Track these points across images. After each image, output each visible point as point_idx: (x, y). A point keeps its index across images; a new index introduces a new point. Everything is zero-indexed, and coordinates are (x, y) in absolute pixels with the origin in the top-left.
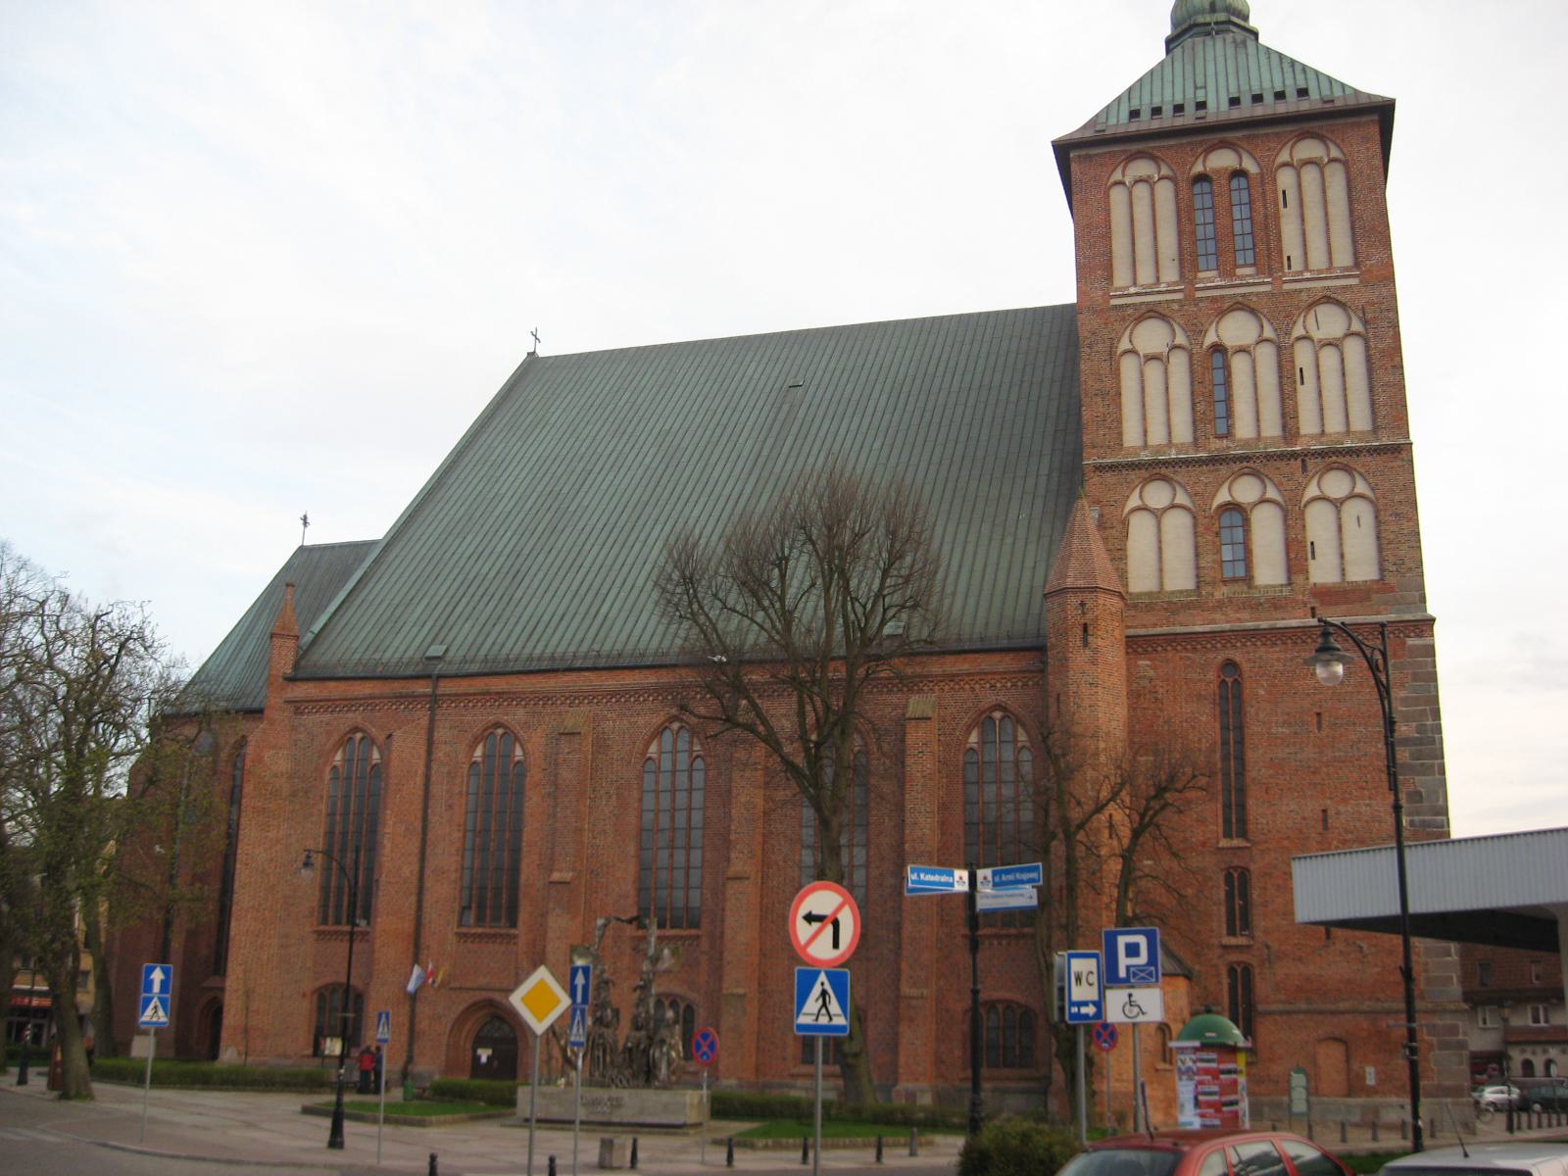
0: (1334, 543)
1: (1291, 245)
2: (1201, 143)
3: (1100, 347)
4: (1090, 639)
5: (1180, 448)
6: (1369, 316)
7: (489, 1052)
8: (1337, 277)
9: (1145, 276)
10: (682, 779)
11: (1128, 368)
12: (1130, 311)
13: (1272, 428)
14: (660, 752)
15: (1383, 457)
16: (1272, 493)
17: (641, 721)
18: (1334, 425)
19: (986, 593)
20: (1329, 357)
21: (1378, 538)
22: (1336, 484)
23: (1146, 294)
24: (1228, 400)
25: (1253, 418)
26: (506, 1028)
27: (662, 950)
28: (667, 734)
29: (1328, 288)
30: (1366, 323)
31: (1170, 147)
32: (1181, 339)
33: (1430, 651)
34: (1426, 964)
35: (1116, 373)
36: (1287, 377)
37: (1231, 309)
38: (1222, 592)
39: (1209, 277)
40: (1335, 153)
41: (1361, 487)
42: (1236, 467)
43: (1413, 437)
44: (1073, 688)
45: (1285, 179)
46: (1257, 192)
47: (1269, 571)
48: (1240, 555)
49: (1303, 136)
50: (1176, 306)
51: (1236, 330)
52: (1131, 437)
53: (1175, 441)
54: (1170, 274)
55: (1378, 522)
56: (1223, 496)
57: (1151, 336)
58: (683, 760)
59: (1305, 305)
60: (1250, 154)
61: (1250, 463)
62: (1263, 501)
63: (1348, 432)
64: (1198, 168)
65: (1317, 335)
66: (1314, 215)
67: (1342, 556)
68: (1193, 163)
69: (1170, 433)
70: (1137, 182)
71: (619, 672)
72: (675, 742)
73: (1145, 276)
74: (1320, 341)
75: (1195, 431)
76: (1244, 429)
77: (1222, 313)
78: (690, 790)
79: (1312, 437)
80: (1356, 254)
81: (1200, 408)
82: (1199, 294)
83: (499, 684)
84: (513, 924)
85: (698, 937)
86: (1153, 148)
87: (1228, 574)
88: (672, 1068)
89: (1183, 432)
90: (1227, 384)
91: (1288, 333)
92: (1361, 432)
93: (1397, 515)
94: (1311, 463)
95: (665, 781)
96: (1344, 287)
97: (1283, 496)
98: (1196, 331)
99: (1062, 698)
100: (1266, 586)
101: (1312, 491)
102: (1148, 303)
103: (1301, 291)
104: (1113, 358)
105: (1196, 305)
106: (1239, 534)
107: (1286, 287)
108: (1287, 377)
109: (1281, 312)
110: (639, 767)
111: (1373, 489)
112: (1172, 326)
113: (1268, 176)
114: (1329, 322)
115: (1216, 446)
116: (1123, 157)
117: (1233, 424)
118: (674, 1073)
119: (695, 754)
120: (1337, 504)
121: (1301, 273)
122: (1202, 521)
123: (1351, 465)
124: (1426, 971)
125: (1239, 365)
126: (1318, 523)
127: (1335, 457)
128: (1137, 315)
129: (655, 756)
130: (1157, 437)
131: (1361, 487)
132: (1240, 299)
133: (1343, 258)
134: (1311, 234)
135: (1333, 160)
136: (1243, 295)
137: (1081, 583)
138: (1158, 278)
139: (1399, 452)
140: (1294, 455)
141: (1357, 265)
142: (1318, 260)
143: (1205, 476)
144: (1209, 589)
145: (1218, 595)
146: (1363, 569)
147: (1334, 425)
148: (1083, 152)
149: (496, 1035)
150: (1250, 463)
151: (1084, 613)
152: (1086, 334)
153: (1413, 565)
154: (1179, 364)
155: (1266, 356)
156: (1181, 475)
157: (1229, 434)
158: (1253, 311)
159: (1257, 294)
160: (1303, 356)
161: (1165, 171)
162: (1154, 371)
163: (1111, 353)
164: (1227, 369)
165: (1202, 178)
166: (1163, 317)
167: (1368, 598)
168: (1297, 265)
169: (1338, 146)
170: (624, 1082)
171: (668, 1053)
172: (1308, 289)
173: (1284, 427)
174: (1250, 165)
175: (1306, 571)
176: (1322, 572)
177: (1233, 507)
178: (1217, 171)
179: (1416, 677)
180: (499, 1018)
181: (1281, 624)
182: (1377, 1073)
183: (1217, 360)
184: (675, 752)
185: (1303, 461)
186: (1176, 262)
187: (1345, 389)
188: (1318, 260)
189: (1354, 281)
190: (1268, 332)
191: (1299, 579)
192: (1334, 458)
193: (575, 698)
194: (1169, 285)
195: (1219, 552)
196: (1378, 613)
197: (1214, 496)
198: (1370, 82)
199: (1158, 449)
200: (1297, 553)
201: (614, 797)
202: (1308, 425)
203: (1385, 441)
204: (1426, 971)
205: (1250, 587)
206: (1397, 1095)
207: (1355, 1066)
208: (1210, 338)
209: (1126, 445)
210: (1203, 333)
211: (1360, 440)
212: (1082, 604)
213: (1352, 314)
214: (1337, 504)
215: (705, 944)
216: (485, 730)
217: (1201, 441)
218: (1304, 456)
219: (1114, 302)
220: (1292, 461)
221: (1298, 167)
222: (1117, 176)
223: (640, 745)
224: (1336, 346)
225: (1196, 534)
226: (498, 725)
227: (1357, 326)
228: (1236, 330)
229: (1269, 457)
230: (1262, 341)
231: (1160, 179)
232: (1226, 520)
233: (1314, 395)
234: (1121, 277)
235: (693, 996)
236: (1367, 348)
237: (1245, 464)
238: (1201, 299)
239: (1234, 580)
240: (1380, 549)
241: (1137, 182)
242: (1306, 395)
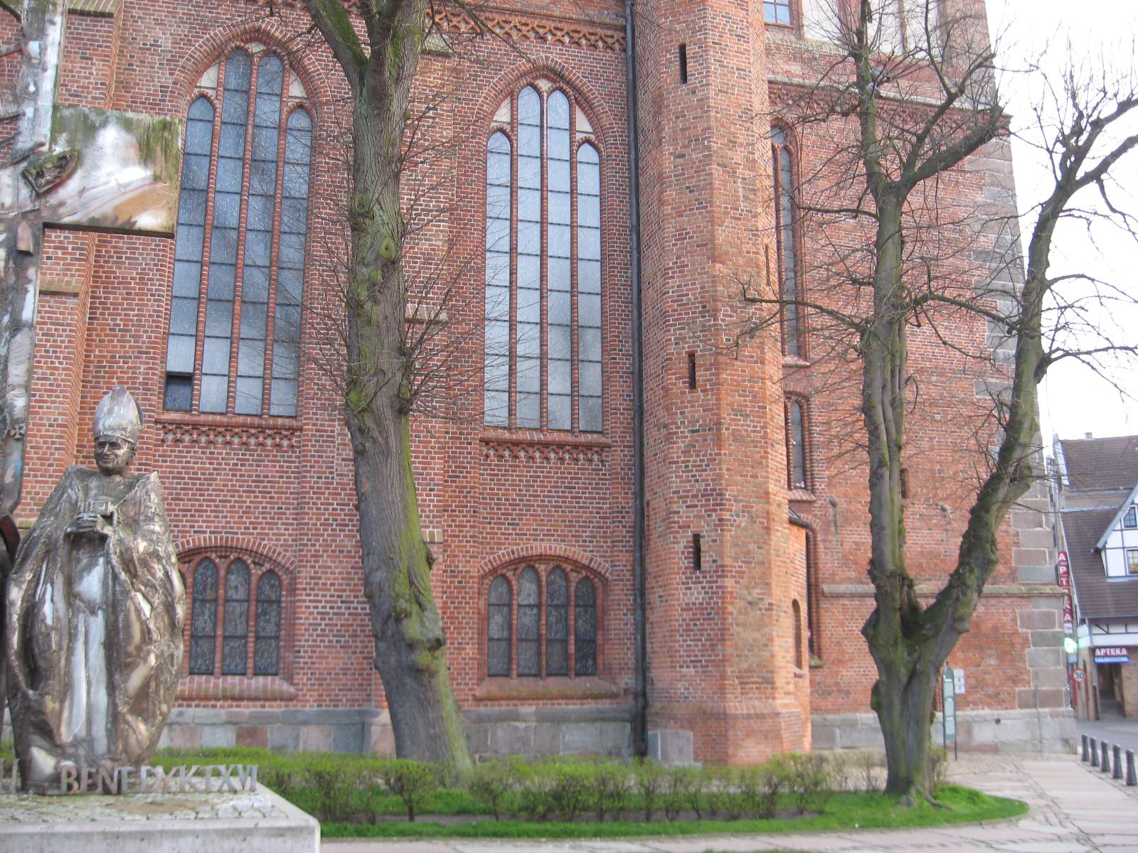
27: (90, 130)
34: (1017, 534)
44: (712, 37)
88: (136, 679)
118: (142, 703)
124: (1017, 544)
171: (114, 607)
182: (967, 677)
204: (1017, 544)
205: (800, 37)
206: (990, 706)
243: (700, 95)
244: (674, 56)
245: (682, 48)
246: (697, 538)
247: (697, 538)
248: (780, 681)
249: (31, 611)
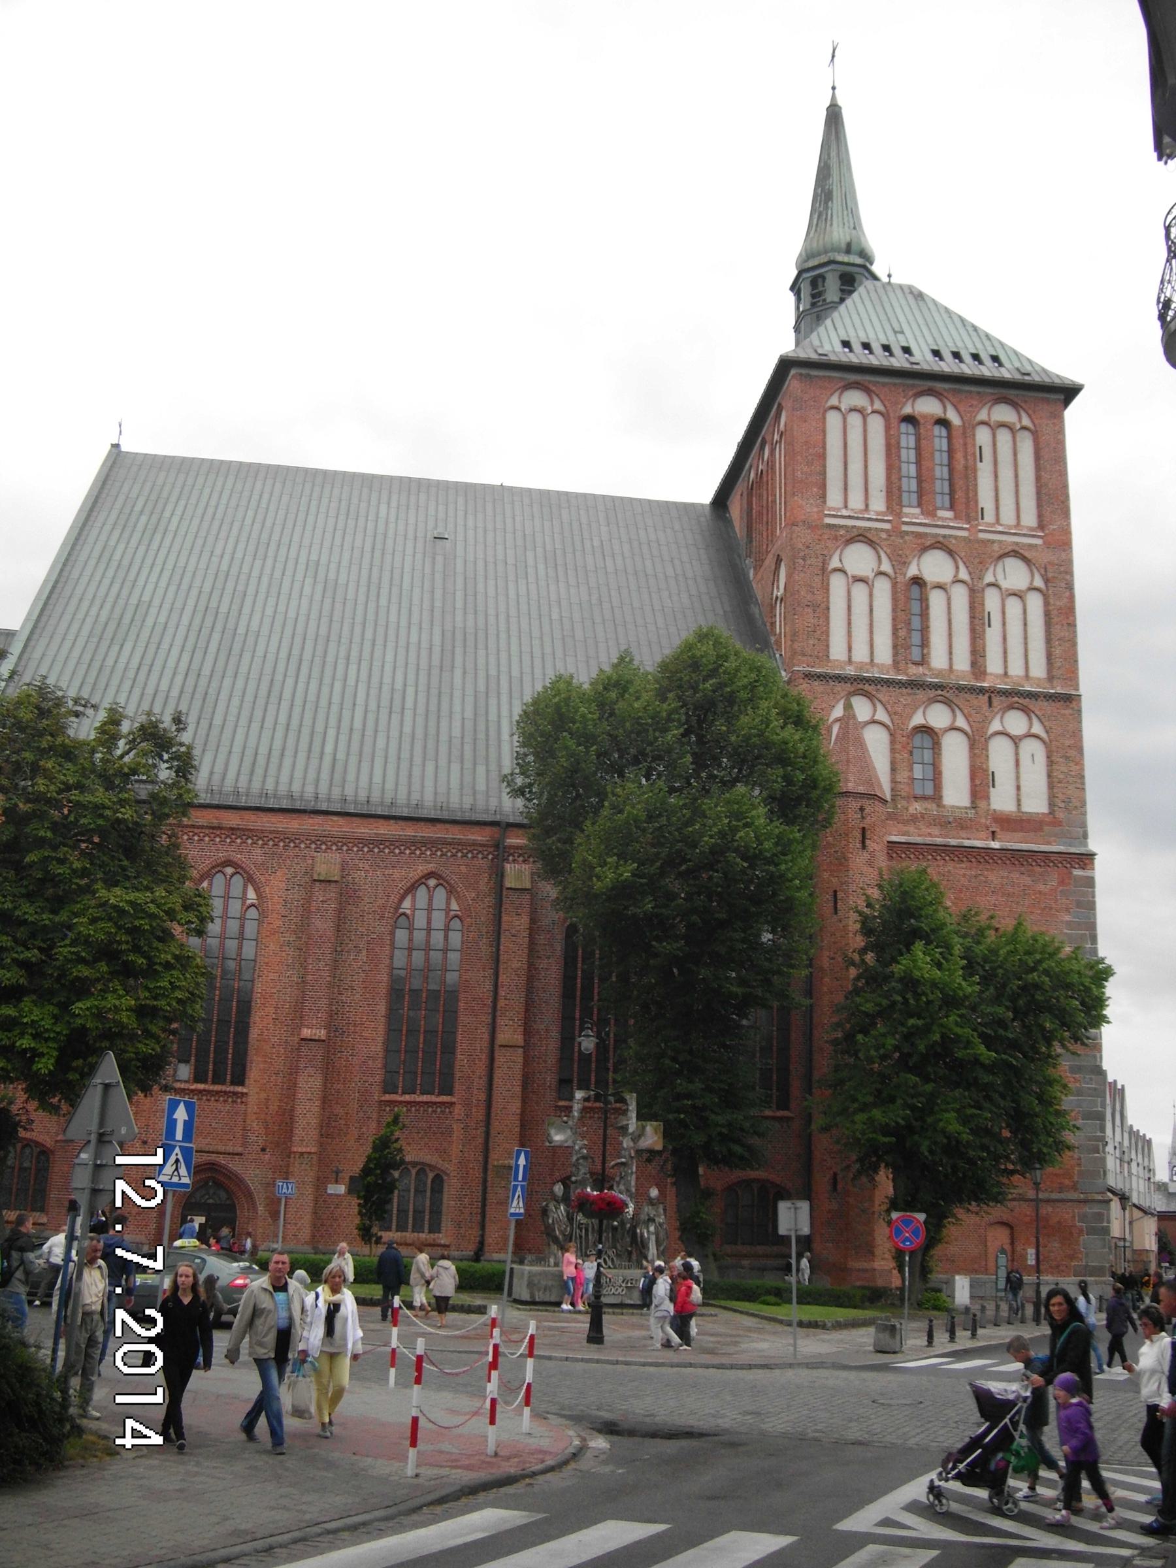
0: (1013, 775)
1: (985, 499)
2: (913, 386)
3: (813, 561)
4: (868, 842)
5: (881, 667)
6: (1050, 575)
7: (203, 1220)
8: (1024, 535)
9: (856, 501)
10: (437, 938)
11: (837, 584)
12: (842, 532)
13: (962, 663)
14: (414, 909)
15: (1055, 703)
16: (961, 722)
17: (396, 874)
18: (1016, 670)
19: (237, 749)
20: (1013, 605)
21: (1049, 776)
22: (1016, 723)
23: (858, 518)
24: (925, 630)
25: (947, 653)
26: (223, 1195)
28: (422, 892)
29: (1017, 544)
30: (1047, 581)
31: (884, 385)
32: (886, 567)
33: (1090, 882)
34: (1080, 1159)
35: (826, 588)
36: (978, 620)
37: (932, 547)
38: (916, 807)
39: (912, 513)
40: (1026, 421)
41: (1037, 728)
42: (932, 693)
43: (1083, 690)
45: (983, 436)
46: (958, 443)
47: (956, 794)
48: (930, 776)
49: (930, 392)
50: (884, 536)
51: (934, 567)
52: (837, 651)
53: (854, 659)
54: (878, 504)
55: (1050, 763)
56: (917, 720)
57: (859, 559)
58: (438, 920)
59: (997, 555)
60: (955, 406)
61: (944, 691)
62: (954, 728)
63: (1027, 676)
64: (907, 410)
65: (1004, 584)
66: (1006, 473)
67: (1018, 788)
68: (905, 404)
69: (872, 653)
70: (851, 410)
71: (372, 820)
72: (431, 899)
73: (856, 501)
74: (1007, 590)
75: (895, 655)
76: (938, 660)
77: (925, 549)
78: (445, 951)
79: (997, 676)
80: (1040, 516)
81: (902, 633)
82: (905, 528)
83: (232, 820)
84: (239, 1079)
85: (452, 1104)
86: (870, 382)
87: (918, 791)
89: (884, 655)
90: (924, 614)
91: (981, 578)
92: (1039, 679)
93: (1067, 758)
94: (996, 700)
95: (420, 937)
96: (1030, 545)
97: (971, 727)
98: (900, 562)
99: (840, 895)
100: (953, 807)
101: (995, 726)
102: (859, 528)
103: (993, 542)
104: (824, 572)
105: (902, 537)
106: (928, 756)
107: (981, 536)
108: (978, 620)
109: (977, 556)
110: (391, 922)
111: (1047, 732)
112: (878, 553)
113: (969, 429)
114: (1014, 575)
115: (915, 671)
116: (842, 384)
117: (929, 653)
119: (452, 913)
120: (1016, 741)
121: (993, 525)
122: (900, 739)
123: (1031, 707)
124: (1079, 1165)
125: (936, 600)
126: (999, 755)
127: (1017, 698)
128: (848, 537)
129: (408, 912)
130: (861, 654)
131: (1037, 728)
132: (941, 539)
133: (1029, 518)
134: (1003, 491)
135: (1024, 428)
136: (944, 536)
137: (861, 789)
138: (867, 506)
139: (1069, 700)
140: (982, 691)
141: (1041, 526)
142: (1008, 517)
143: (904, 697)
144: (904, 803)
145: (911, 810)
146: (1036, 803)
147: (1016, 670)
148: (804, 371)
149: (211, 1201)
150: (944, 691)
151: (863, 818)
152: (800, 546)
153: (1078, 804)
154: (883, 589)
155: (960, 595)
156: (883, 693)
157: (924, 661)
158: (951, 553)
159: (956, 537)
160: (992, 601)
161: (878, 405)
162: (860, 591)
163: (823, 569)
164: (924, 602)
165: (910, 419)
166: (871, 543)
167: (1041, 830)
168: (989, 517)
169: (1030, 416)
170: (610, 1263)
172: (1000, 542)
173: (974, 664)
174: (953, 416)
175: (987, 797)
176: (1001, 800)
177: (925, 730)
178: (925, 416)
179: (1079, 904)
180: (218, 1185)
181: (967, 843)
183: (915, 590)
184: (430, 909)
185: (990, 698)
186: (884, 494)
187: (1026, 638)
188: (1008, 517)
189: (1039, 542)
190: (964, 574)
191: (982, 804)
192: (1016, 699)
193: (321, 842)
194: (878, 513)
195: (911, 770)
196: (1049, 843)
197: (910, 717)
198: (1058, 365)
199: (861, 666)
200: (981, 780)
201: (364, 952)
202: (994, 665)
203: (1059, 690)
204: (1079, 1165)
205: (940, 805)
206: (1052, 1274)
207: (1019, 1249)
208: (912, 571)
209: (831, 658)
210: (906, 564)
211: (1038, 686)
212: (862, 809)
213: (1035, 571)
214: (1016, 741)
215: (458, 1110)
216: (213, 867)
217: (902, 665)
218: (991, 693)
219: (828, 521)
220: (980, 696)
221: (995, 427)
222: (834, 401)
223: (394, 898)
224: (1020, 597)
225: (893, 751)
226: (228, 863)
227: (1039, 582)
228: (934, 567)
229: (960, 689)
230: (957, 581)
231: (873, 412)
232: (918, 740)
233: (999, 639)
234: (834, 498)
235: (445, 1166)
236: (1046, 604)
237: (939, 692)
238: (907, 533)
239: (925, 798)
240: (1051, 786)
241: (851, 410)
242: (992, 636)
243: (844, 923)
244: (829, 897)
245: (835, 892)
246: (835, 1174)
247: (835, 1174)
248: (878, 1252)
249: (642, 1234)
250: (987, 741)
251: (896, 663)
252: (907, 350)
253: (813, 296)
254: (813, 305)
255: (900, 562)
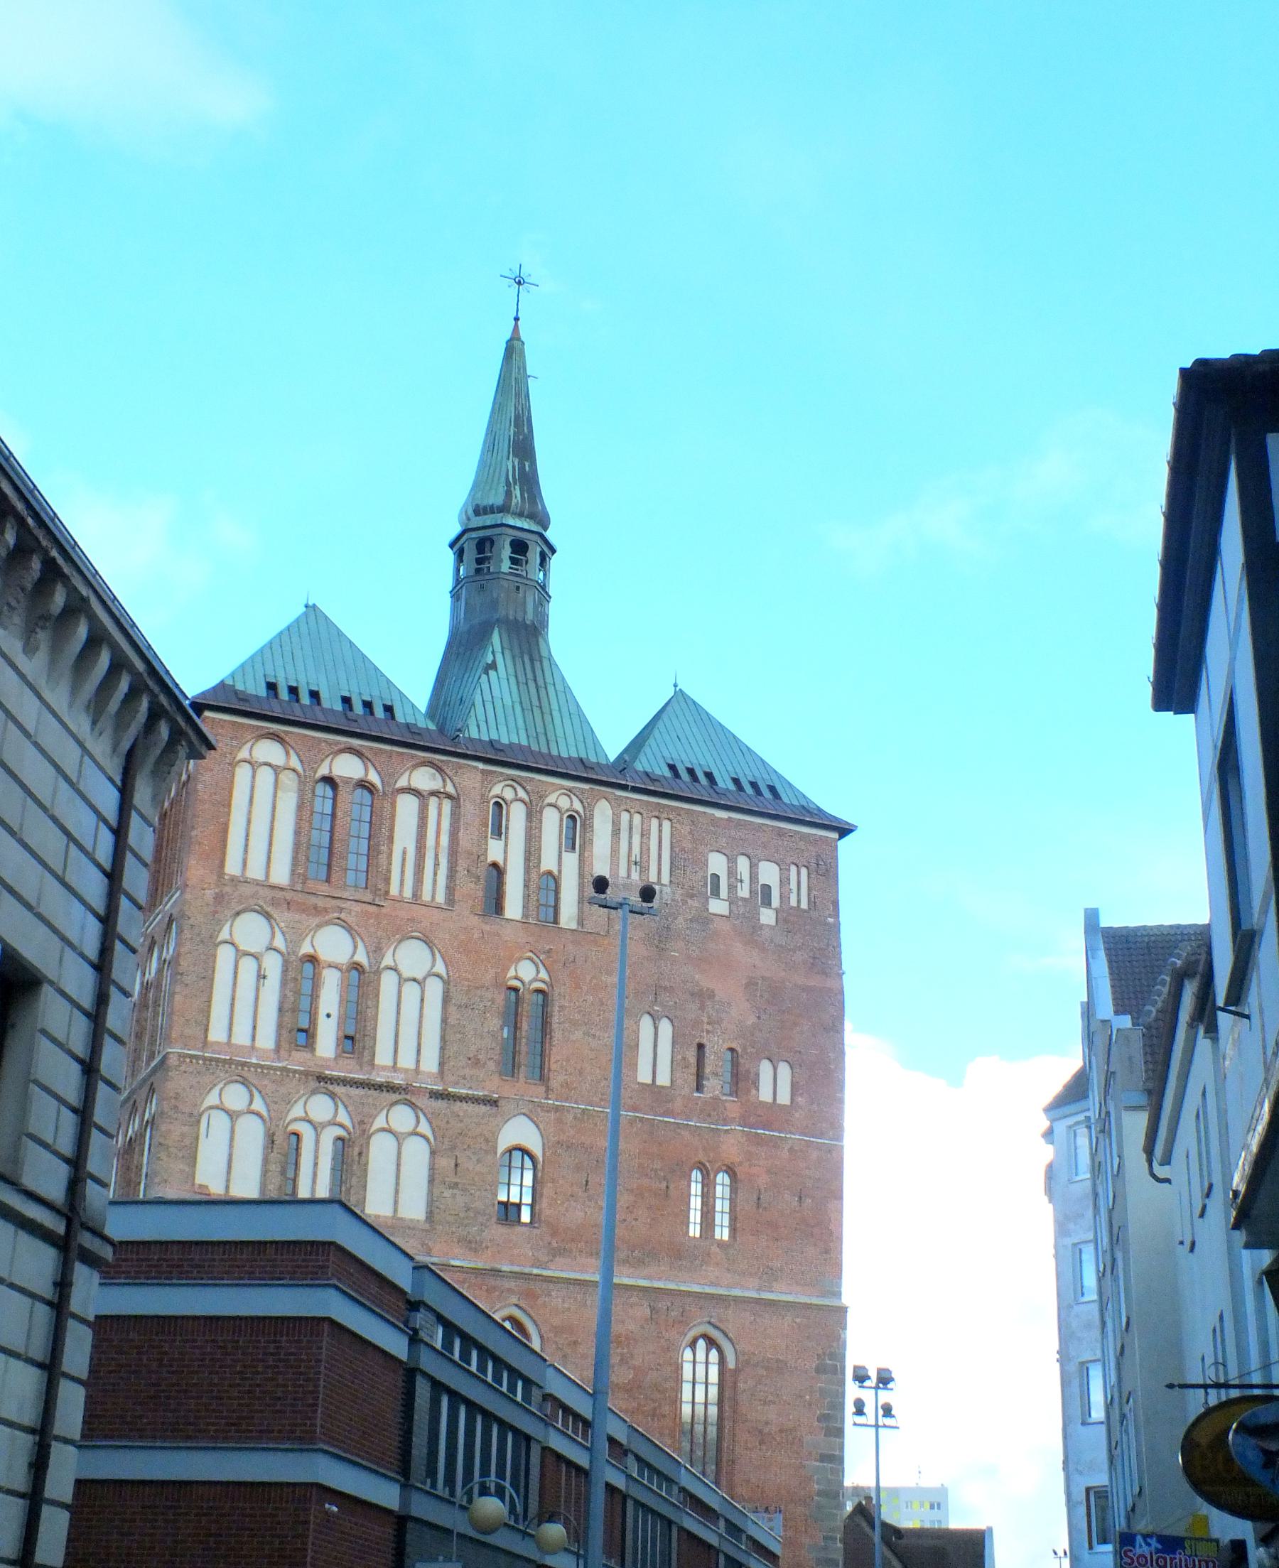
18: (406, 1061)
22: (402, 1118)
32: (279, 942)
52: (217, 1034)
86: (286, 733)
98: (294, 938)
126: (380, 1151)
147: (406, 1061)
208: (306, 949)
210: (299, 943)
250: (369, 1137)
251: (278, 1049)
252: (315, 695)
253: (479, 561)
254: (478, 571)
255: (294, 938)
